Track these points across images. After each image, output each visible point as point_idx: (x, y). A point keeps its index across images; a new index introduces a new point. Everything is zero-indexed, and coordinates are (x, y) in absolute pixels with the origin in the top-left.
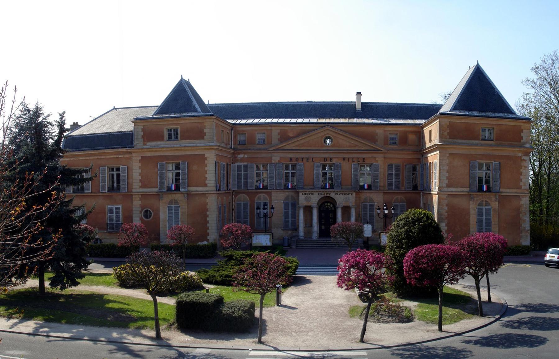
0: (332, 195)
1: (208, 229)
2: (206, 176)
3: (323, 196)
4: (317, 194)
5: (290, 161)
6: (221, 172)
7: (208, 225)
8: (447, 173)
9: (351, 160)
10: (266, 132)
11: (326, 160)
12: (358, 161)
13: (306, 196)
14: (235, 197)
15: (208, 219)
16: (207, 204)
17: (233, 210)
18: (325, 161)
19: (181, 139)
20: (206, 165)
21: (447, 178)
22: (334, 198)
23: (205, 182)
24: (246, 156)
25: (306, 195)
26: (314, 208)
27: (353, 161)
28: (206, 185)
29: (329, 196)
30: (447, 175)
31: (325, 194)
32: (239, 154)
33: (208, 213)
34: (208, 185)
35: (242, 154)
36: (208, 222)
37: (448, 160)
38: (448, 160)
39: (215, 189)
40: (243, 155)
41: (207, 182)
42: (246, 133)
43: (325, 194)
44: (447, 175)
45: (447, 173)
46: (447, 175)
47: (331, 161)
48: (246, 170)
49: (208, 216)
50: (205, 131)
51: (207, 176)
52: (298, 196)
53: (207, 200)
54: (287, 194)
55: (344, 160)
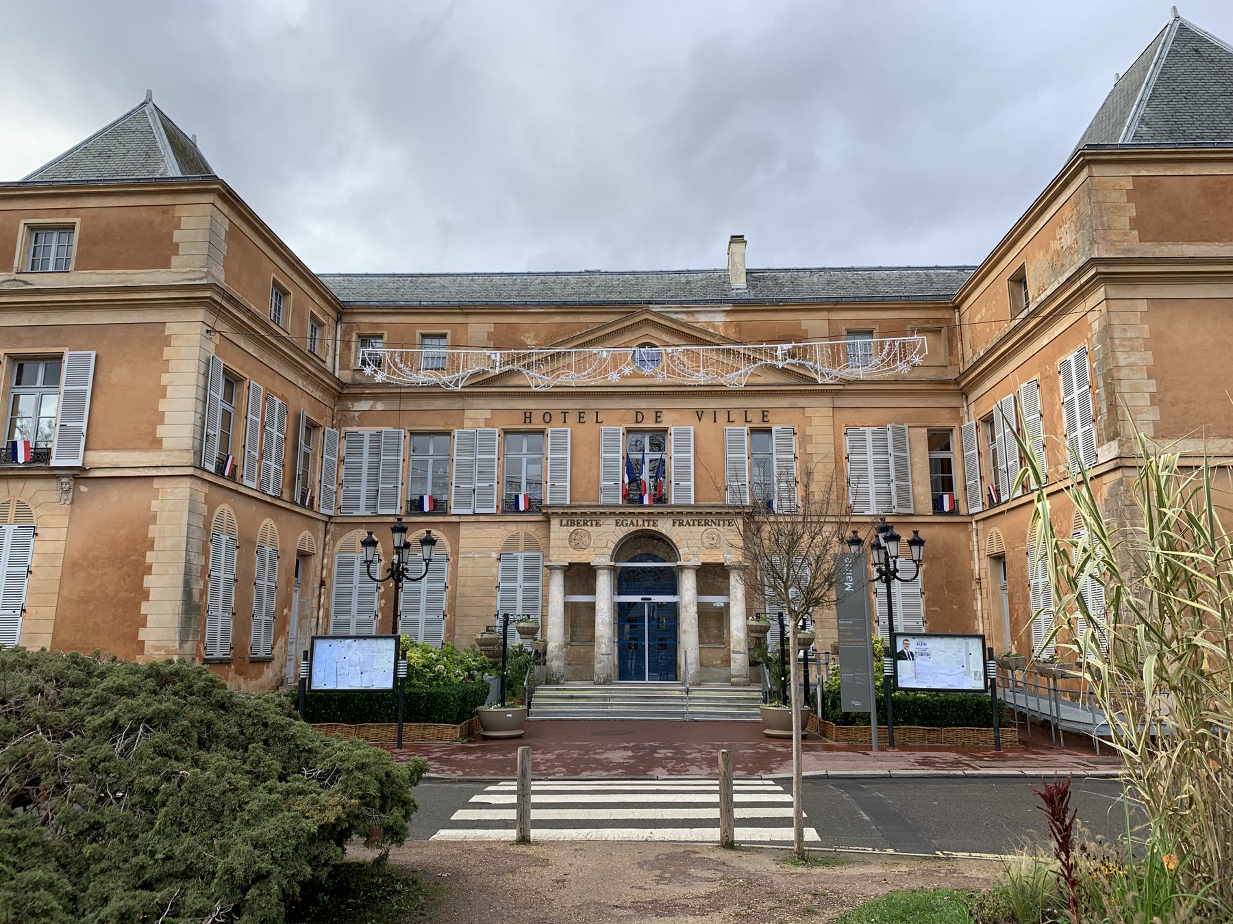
0: (664, 527)
1: (144, 626)
2: (161, 409)
3: (632, 529)
4: (612, 521)
5: (525, 423)
6: (250, 416)
7: (145, 608)
8: (1149, 377)
9: (722, 418)
10: (449, 331)
11: (640, 419)
12: (746, 421)
13: (572, 529)
14: (335, 540)
15: (148, 581)
16: (153, 520)
17: (322, 583)
18: (637, 422)
19: (76, 269)
20: (165, 366)
21: (1154, 400)
22: (668, 535)
23: (154, 431)
24: (380, 406)
25: (575, 527)
26: (599, 572)
27: (729, 421)
28: (156, 443)
29: (653, 528)
30: (1151, 386)
31: (640, 522)
32: (358, 397)
33: (150, 557)
34: (166, 444)
35: (367, 399)
36: (146, 595)
37: (1146, 327)
38: (1146, 327)
39: (189, 458)
40: (371, 402)
41: (161, 431)
42: (386, 333)
43: (640, 522)
44: (1154, 390)
45: (1149, 377)
46: (1151, 386)
47: (656, 422)
48: (375, 452)
49: (148, 570)
50: (177, 236)
51: (163, 406)
52: (548, 537)
53: (155, 505)
54: (513, 529)
55: (700, 420)
